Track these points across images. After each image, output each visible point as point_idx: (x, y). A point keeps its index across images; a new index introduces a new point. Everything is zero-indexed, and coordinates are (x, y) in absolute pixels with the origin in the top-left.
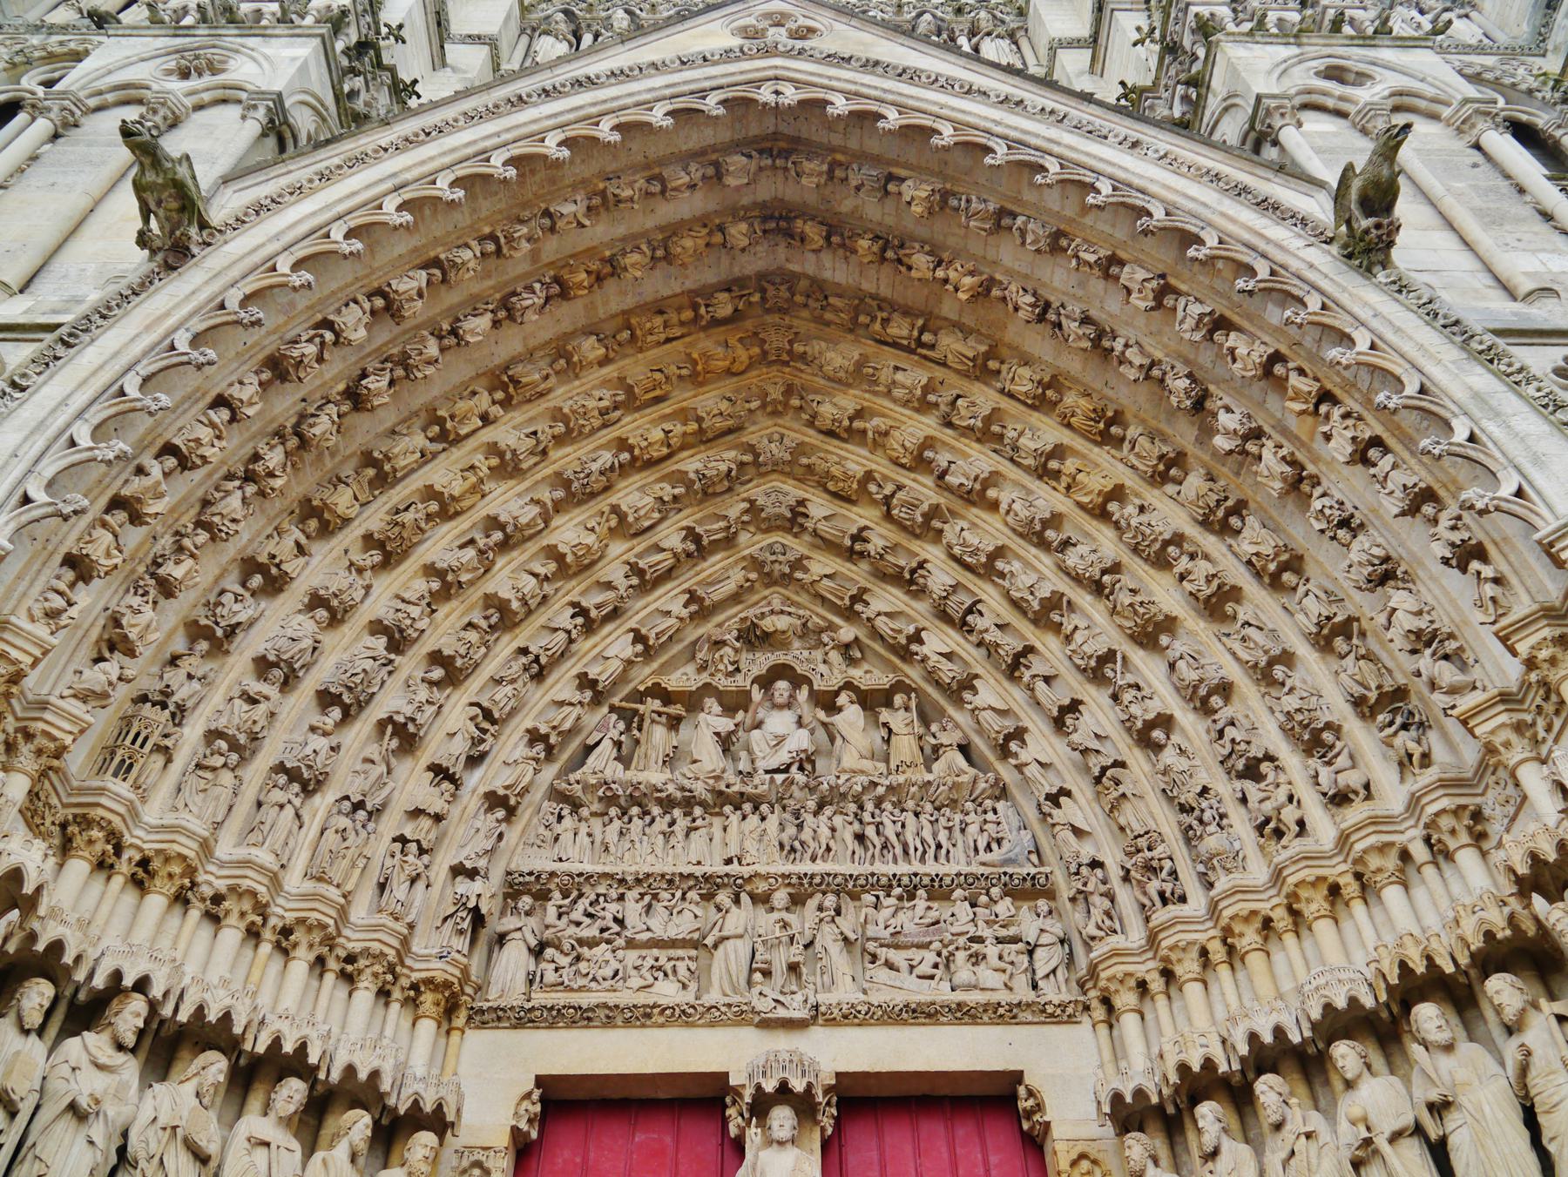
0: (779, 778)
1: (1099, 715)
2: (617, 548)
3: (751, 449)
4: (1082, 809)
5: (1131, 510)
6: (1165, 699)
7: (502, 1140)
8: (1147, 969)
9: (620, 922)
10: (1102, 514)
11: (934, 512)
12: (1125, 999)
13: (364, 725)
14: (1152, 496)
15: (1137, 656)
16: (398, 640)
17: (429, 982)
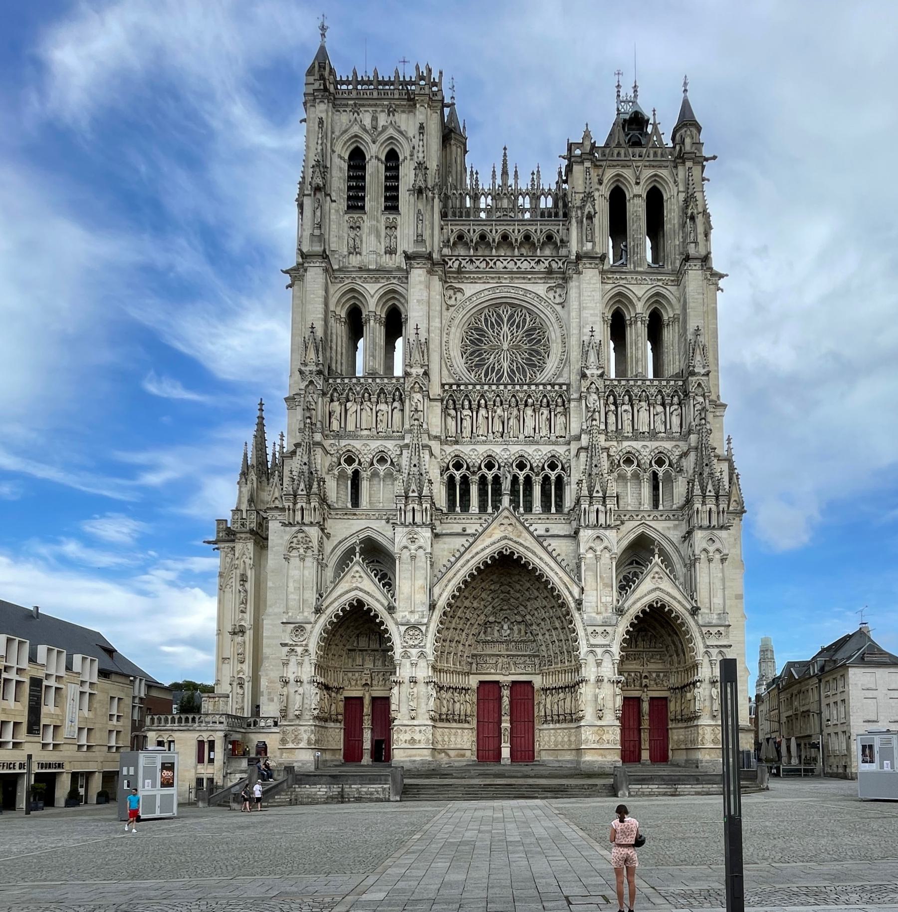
1: (547, 636)
2: (482, 603)
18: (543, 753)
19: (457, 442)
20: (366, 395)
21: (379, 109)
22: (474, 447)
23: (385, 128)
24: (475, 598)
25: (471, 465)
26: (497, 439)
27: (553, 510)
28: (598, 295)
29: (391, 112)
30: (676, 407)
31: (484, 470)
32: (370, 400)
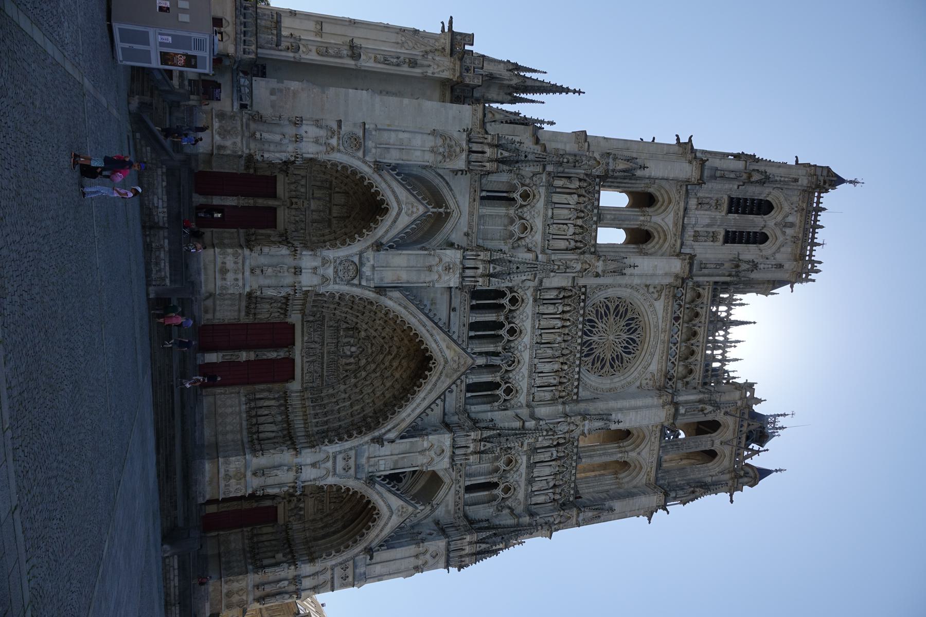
0: (341, 350)
1: (343, 396)
2: (380, 328)
3: (400, 347)
4: (331, 391)
5: (371, 405)
10: (373, 401)
12: (302, 394)
14: (372, 409)
15: (349, 402)
18: (211, 399)
19: (535, 300)
20: (583, 215)
21: (797, 230)
22: (530, 317)
23: (784, 233)
25: (515, 314)
26: (535, 338)
27: (469, 395)
28: (645, 422)
29: (795, 239)
30: (552, 498)
31: (507, 327)
32: (578, 218)
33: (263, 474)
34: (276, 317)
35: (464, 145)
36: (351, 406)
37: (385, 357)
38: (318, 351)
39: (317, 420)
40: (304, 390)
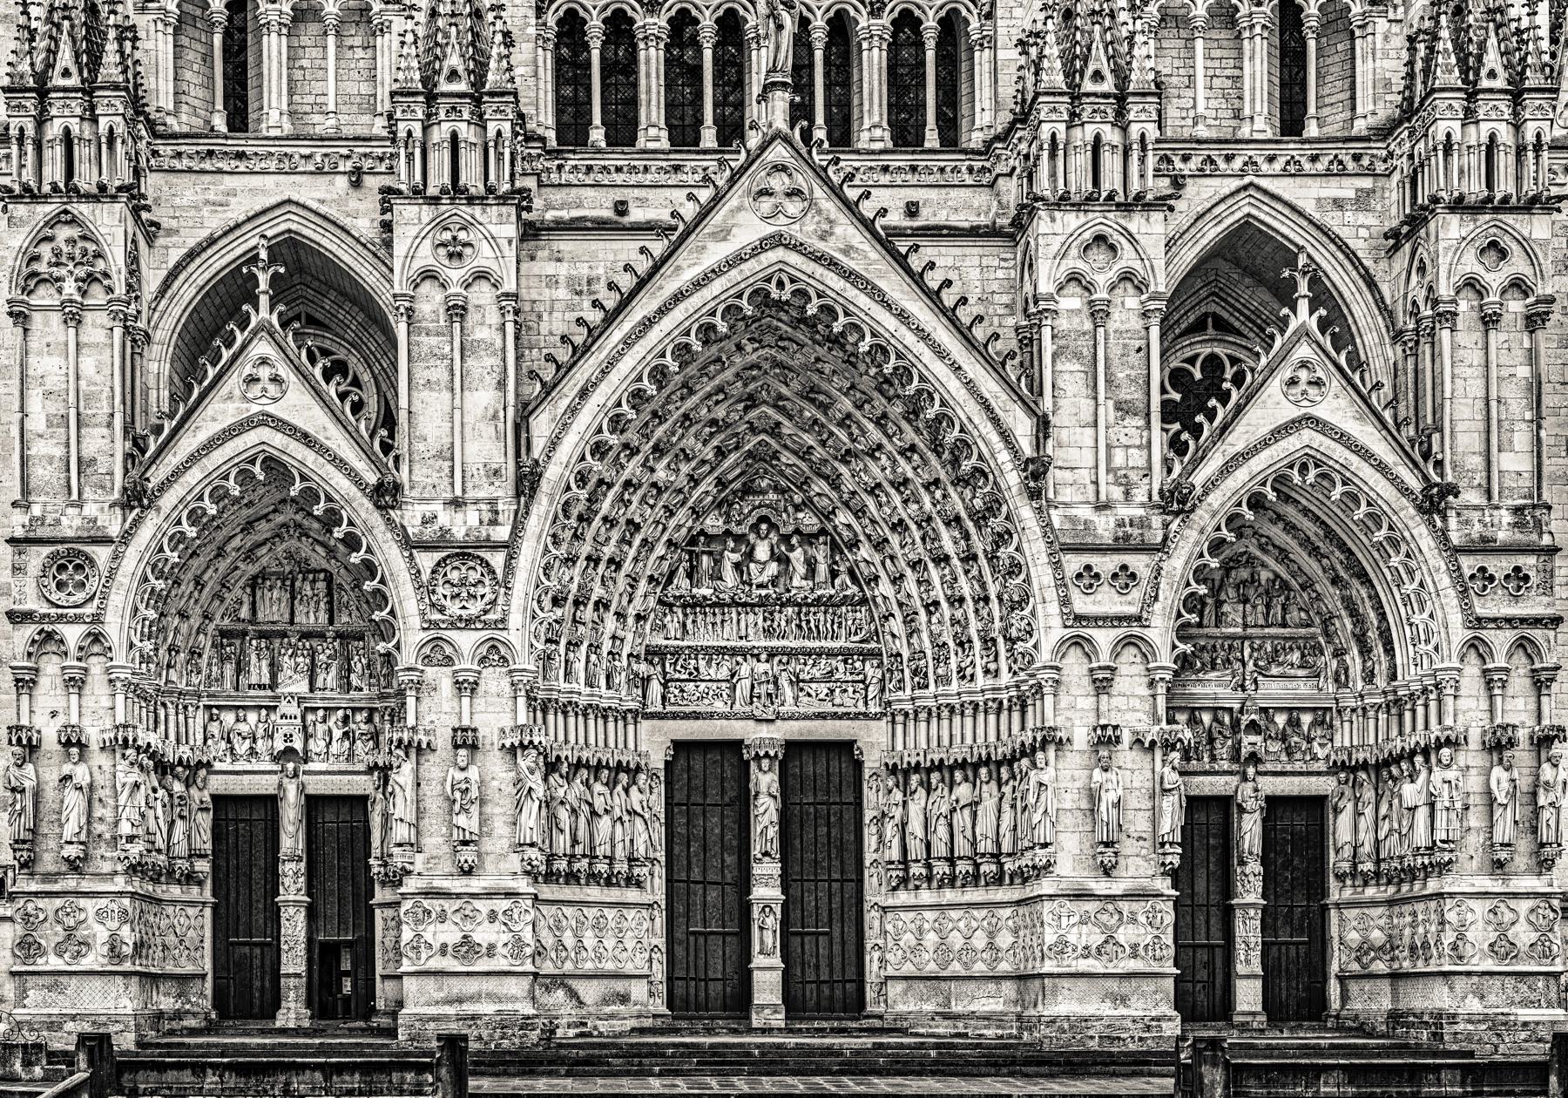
0: (763, 592)
1: (910, 584)
2: (685, 468)
4: (896, 625)
6: (938, 593)
7: (662, 766)
8: (908, 707)
9: (697, 669)
10: (927, 487)
11: (848, 452)
12: (900, 718)
13: (591, 606)
14: (951, 490)
15: (931, 565)
16: (597, 561)
17: (630, 711)
24: (658, 450)
33: (1107, 845)
34: (650, 798)
35: (48, 208)
36: (942, 560)
37: (786, 447)
38: (762, 667)
39: (979, 672)
40: (889, 713)
